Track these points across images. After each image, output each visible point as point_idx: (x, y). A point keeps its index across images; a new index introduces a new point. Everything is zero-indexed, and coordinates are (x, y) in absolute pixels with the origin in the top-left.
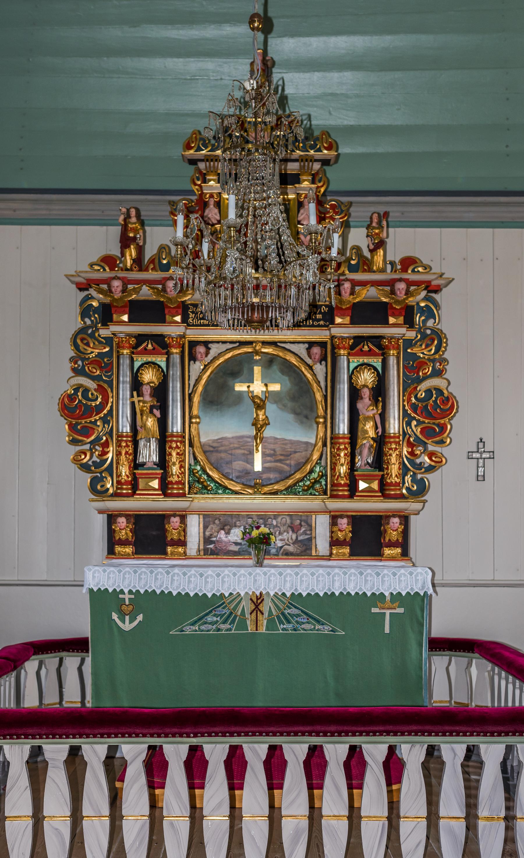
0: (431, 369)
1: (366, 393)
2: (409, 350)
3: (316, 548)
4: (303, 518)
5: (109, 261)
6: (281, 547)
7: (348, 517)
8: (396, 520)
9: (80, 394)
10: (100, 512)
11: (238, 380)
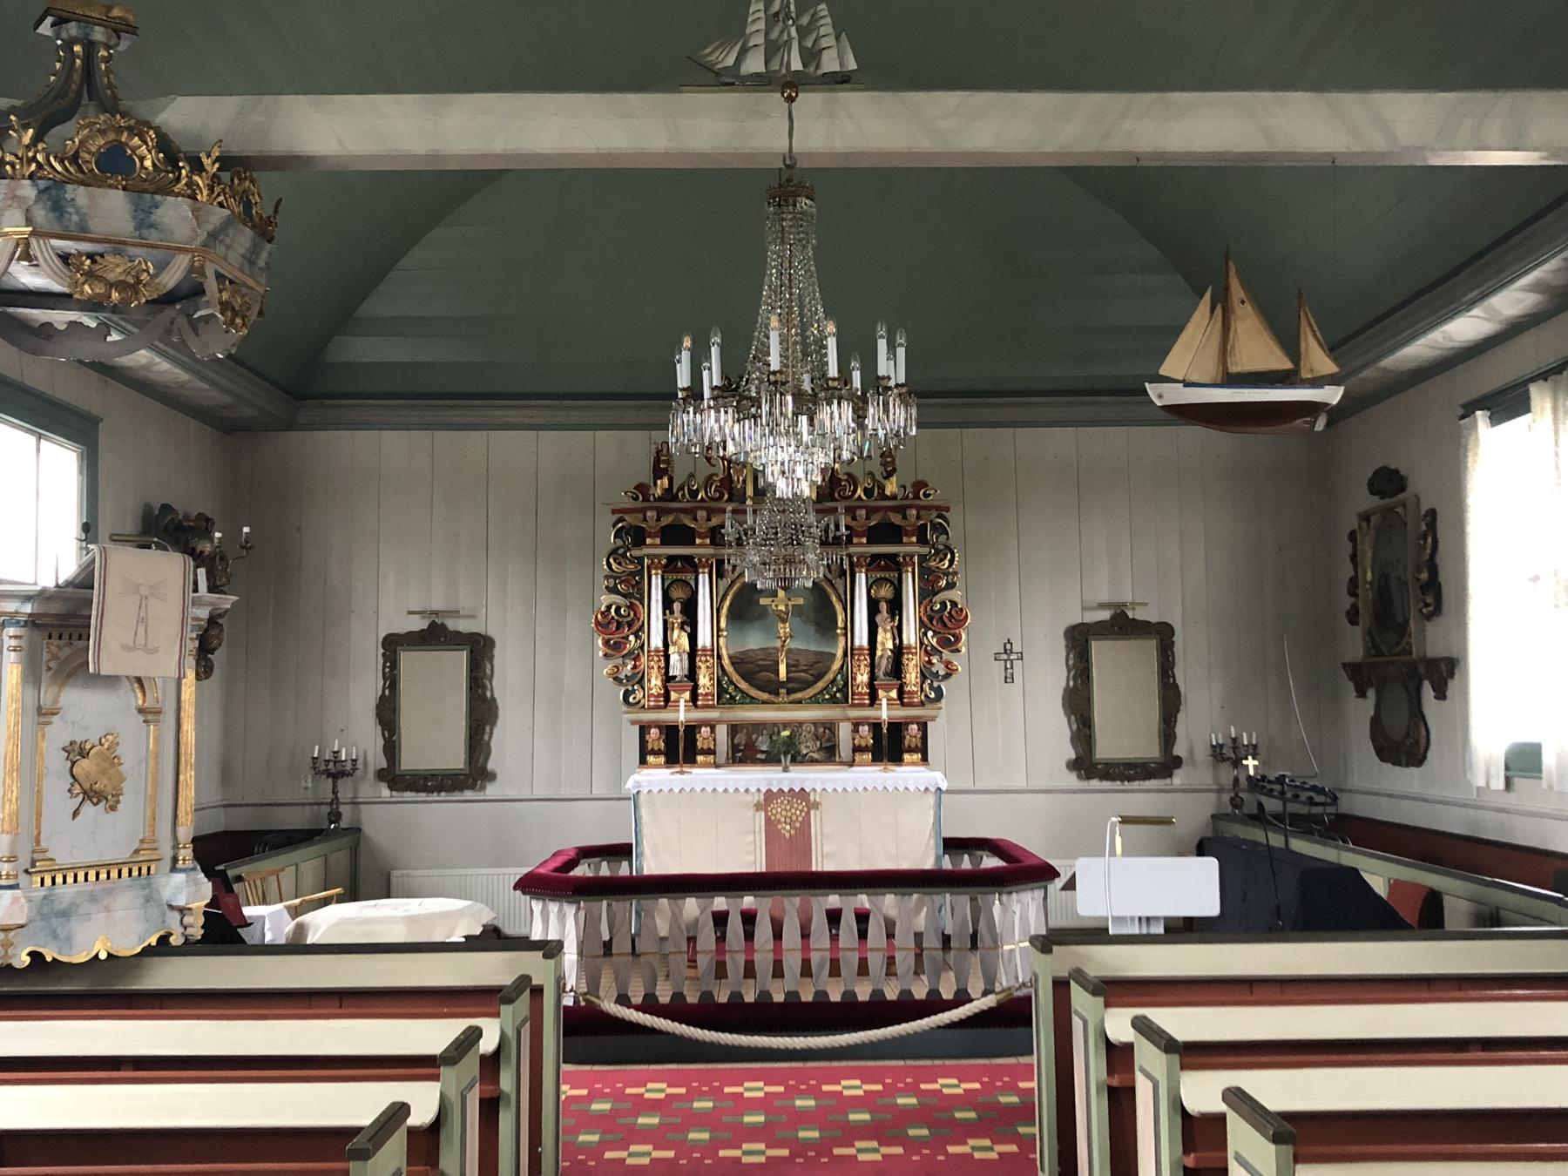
1: (883, 606)
5: (642, 489)
8: (915, 727)
10: (633, 723)
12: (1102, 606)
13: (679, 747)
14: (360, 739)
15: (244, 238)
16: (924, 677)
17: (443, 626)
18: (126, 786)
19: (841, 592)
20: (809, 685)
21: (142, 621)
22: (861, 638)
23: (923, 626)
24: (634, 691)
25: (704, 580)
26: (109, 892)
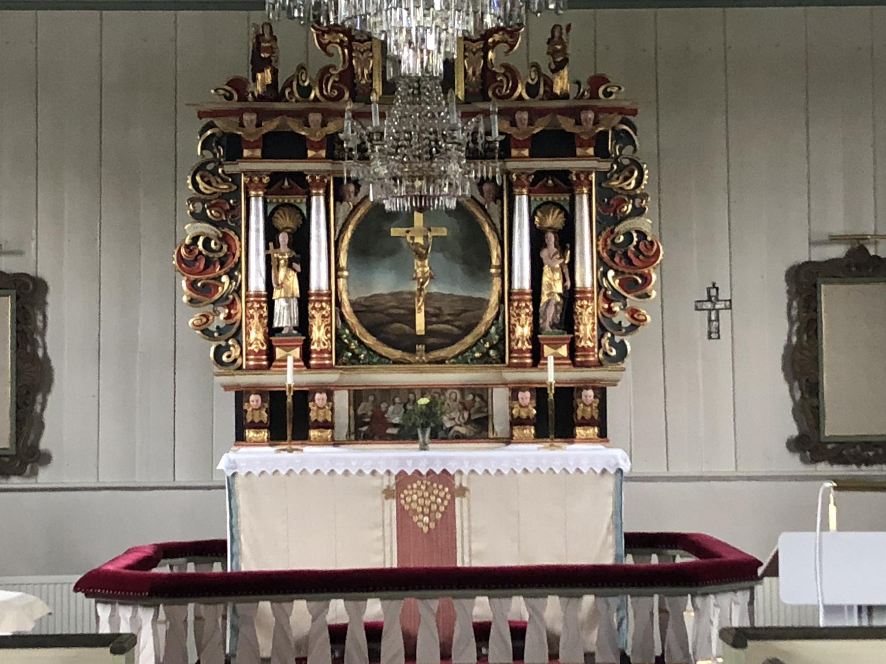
0: (630, 206)
1: (551, 238)
2: (603, 185)
3: (493, 428)
4: (479, 392)
6: (451, 428)
7: (531, 390)
8: (591, 393)
9: (200, 243)
10: (227, 388)
11: (396, 223)
12: (834, 239)
13: (287, 419)
16: (602, 329)
19: (497, 221)
20: (454, 339)
22: (522, 279)
23: (603, 264)
24: (228, 348)
25: (318, 203)
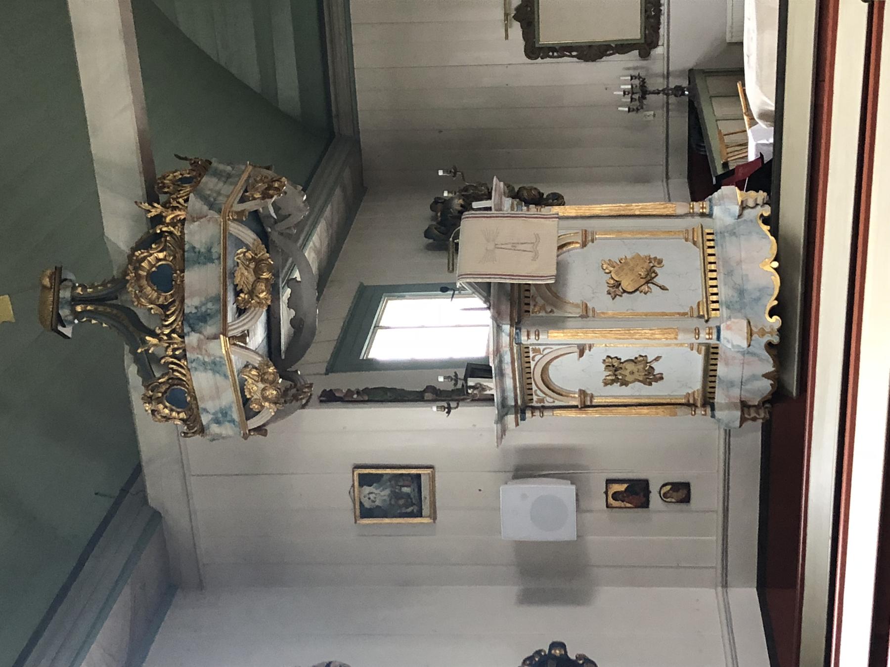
14: (614, 74)
15: (209, 182)
17: (518, 9)
18: (643, 253)
21: (514, 247)
26: (726, 262)
